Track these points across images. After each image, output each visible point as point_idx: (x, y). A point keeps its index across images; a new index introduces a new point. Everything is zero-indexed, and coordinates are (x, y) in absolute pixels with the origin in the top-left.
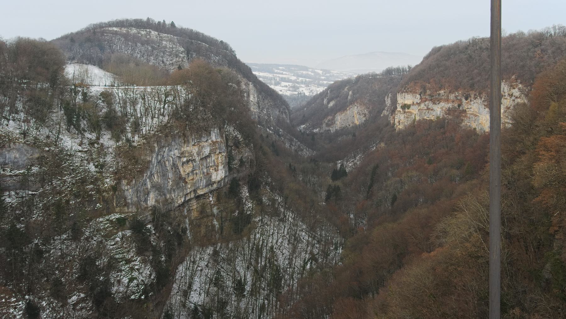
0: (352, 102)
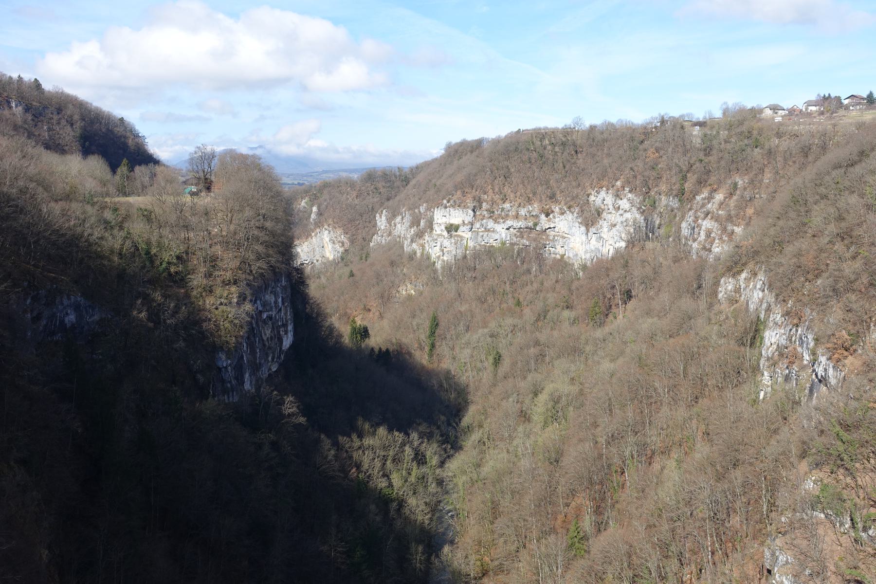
0: (318, 224)
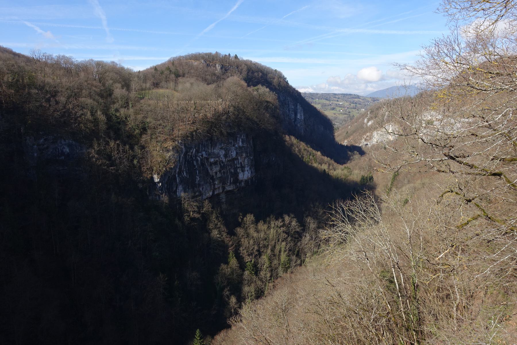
0: (388, 121)
